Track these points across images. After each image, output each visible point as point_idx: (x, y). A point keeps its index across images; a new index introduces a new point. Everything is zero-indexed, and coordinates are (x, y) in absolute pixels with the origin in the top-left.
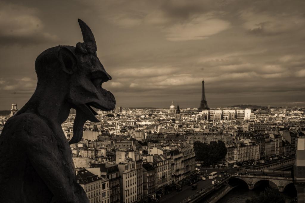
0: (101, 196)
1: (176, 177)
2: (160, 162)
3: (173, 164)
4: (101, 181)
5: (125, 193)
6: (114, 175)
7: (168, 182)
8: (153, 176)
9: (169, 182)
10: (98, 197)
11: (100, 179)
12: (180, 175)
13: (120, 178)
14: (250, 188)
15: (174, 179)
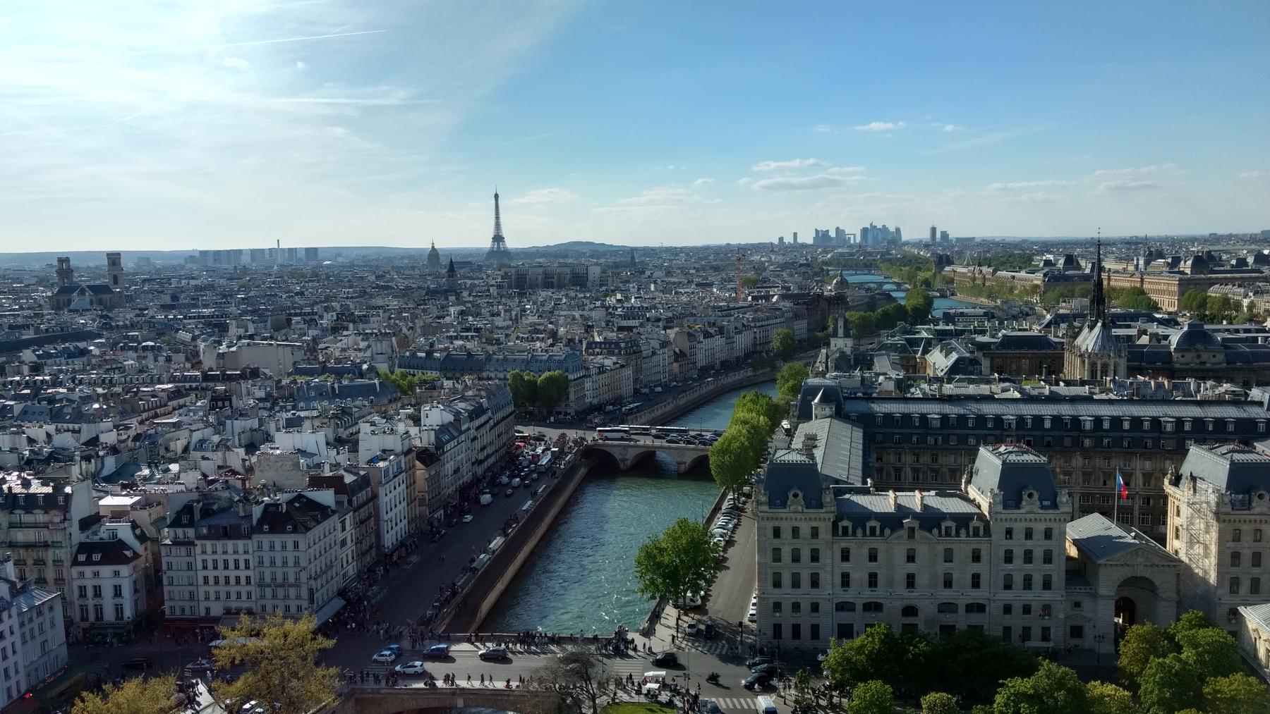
0: (338, 546)
1: (479, 462)
2: (448, 441)
3: (475, 439)
4: (336, 517)
5: (384, 527)
6: (362, 496)
7: (465, 479)
8: (438, 474)
9: (467, 478)
10: (333, 551)
11: (334, 512)
12: (488, 457)
13: (375, 496)
14: (622, 465)
15: (476, 467)
